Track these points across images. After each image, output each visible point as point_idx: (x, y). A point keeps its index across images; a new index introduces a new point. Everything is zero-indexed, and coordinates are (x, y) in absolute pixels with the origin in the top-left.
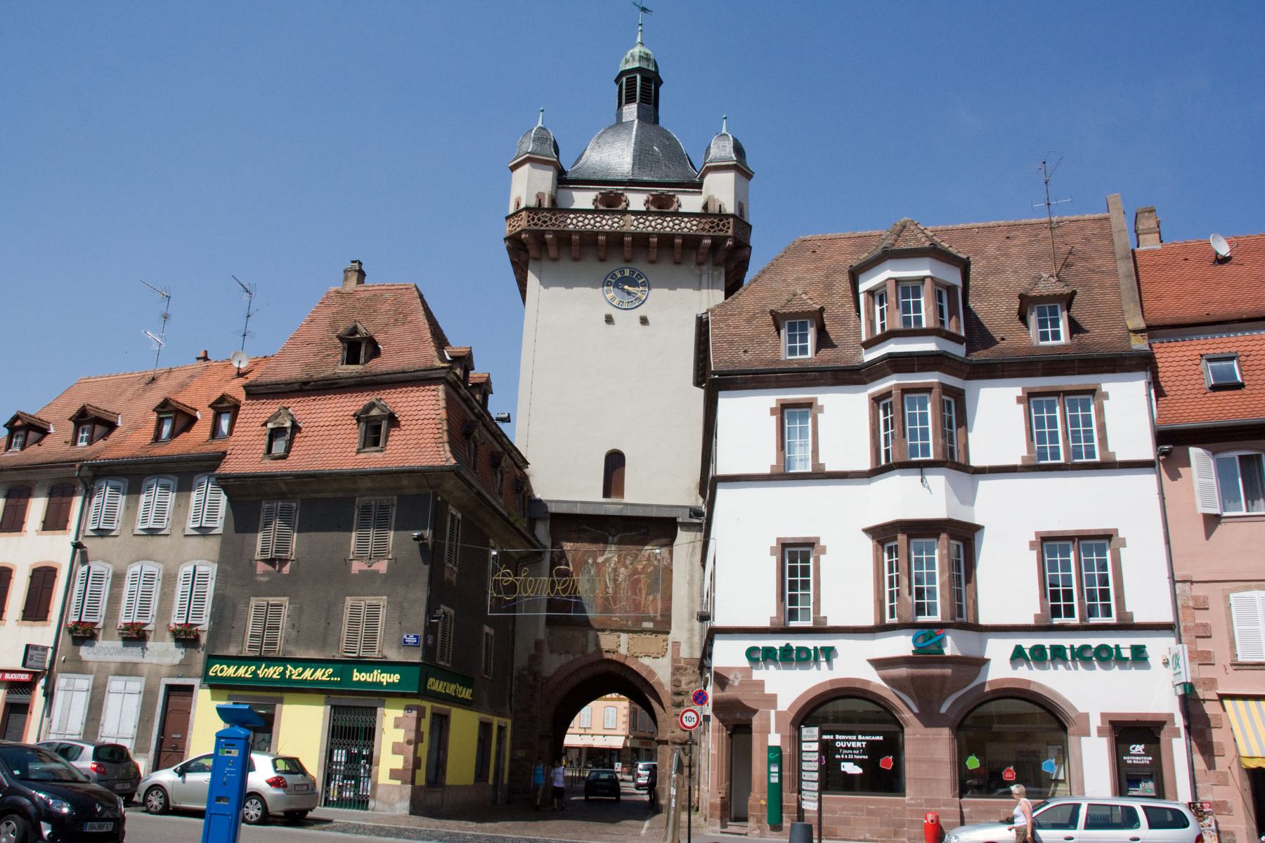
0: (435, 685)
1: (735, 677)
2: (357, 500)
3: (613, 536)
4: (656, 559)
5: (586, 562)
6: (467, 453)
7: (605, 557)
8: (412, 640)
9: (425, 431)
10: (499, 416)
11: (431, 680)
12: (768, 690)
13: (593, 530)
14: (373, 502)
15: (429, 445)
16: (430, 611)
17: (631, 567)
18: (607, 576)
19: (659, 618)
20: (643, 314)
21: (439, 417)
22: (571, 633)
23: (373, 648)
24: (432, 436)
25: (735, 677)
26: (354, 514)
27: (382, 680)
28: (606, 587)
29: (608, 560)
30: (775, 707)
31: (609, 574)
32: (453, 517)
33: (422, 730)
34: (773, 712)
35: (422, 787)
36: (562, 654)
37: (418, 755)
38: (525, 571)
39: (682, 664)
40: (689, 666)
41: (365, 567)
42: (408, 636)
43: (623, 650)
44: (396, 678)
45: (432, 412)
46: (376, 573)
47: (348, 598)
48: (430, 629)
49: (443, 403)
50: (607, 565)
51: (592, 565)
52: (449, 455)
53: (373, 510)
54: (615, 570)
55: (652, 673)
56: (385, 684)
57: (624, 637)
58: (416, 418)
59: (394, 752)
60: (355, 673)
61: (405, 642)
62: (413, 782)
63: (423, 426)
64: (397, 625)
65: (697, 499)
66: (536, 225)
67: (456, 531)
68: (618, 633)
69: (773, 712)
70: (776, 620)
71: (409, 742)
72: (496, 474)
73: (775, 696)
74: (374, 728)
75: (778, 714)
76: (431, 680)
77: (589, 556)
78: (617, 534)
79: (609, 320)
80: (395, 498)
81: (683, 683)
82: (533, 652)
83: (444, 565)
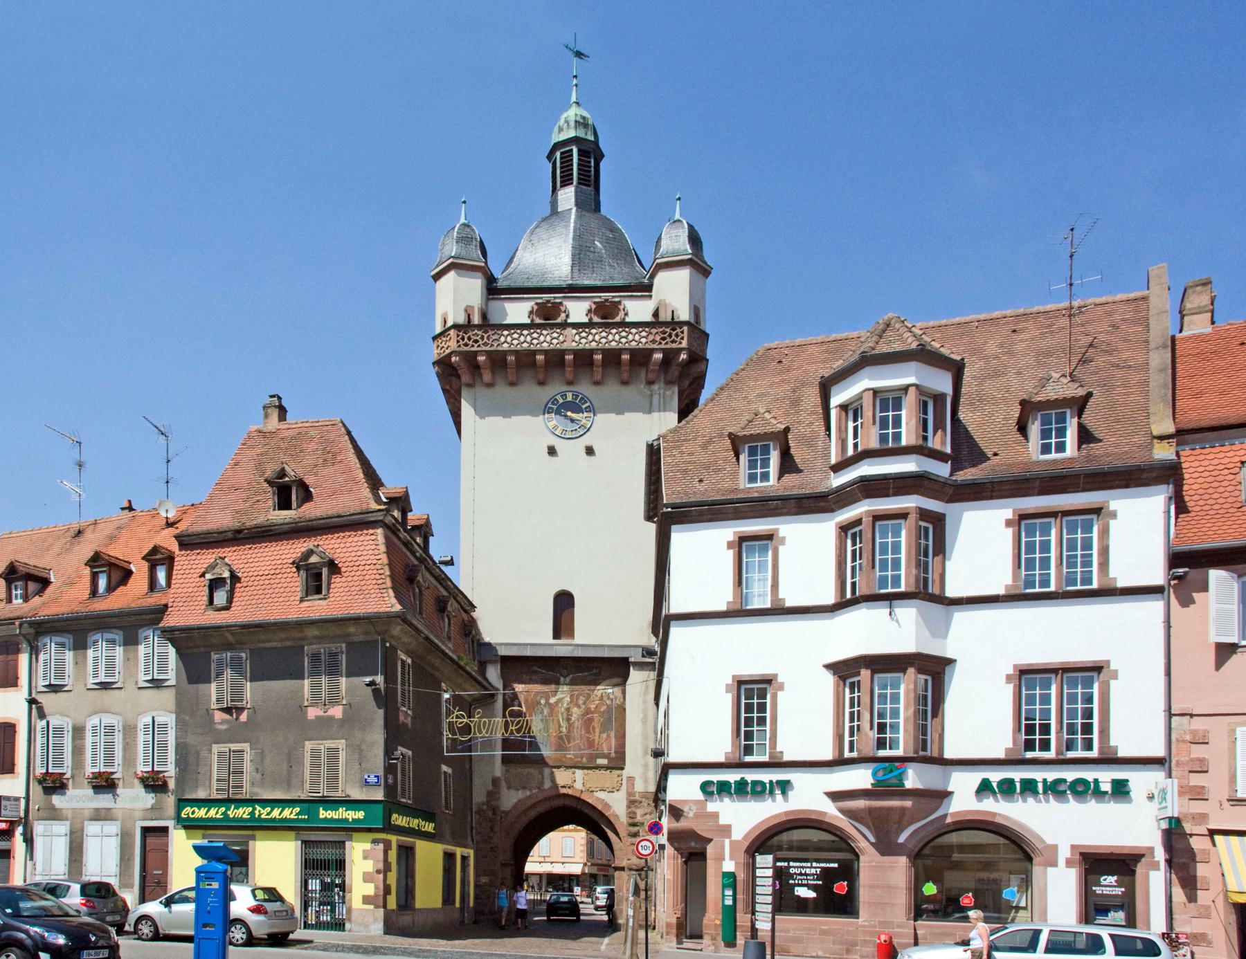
0: (399, 820)
1: (690, 809)
2: (306, 648)
3: (565, 677)
4: (609, 698)
5: (539, 703)
6: (412, 599)
7: (557, 697)
8: (373, 779)
9: (367, 577)
10: (443, 559)
11: (395, 816)
12: (723, 821)
14: (322, 650)
15: (373, 591)
16: (388, 752)
17: (584, 707)
18: (560, 715)
19: (613, 755)
20: (589, 444)
21: (380, 562)
23: (336, 788)
24: (374, 582)
25: (690, 809)
26: (304, 662)
27: (348, 817)
28: (560, 726)
29: (560, 700)
30: (729, 836)
31: (562, 714)
32: (403, 662)
33: (389, 860)
34: (727, 842)
35: (393, 910)
36: (518, 790)
37: (388, 882)
41: (321, 713)
43: (578, 786)
44: (360, 815)
45: (373, 557)
46: (332, 718)
47: (307, 743)
48: (390, 769)
49: (383, 548)
50: (560, 705)
51: (545, 705)
52: (394, 600)
53: (323, 657)
54: (568, 710)
56: (350, 820)
58: (357, 564)
59: (365, 881)
60: (321, 811)
61: (366, 782)
62: (385, 906)
63: (365, 572)
64: (357, 766)
67: (407, 676)
68: (573, 770)
69: (727, 842)
70: (731, 755)
71: (378, 872)
72: (443, 619)
73: (730, 826)
74: (344, 860)
75: (732, 843)
76: (395, 816)
77: (541, 697)
78: (568, 675)
79: (552, 451)
80: (344, 645)
82: (490, 788)
83: (398, 709)
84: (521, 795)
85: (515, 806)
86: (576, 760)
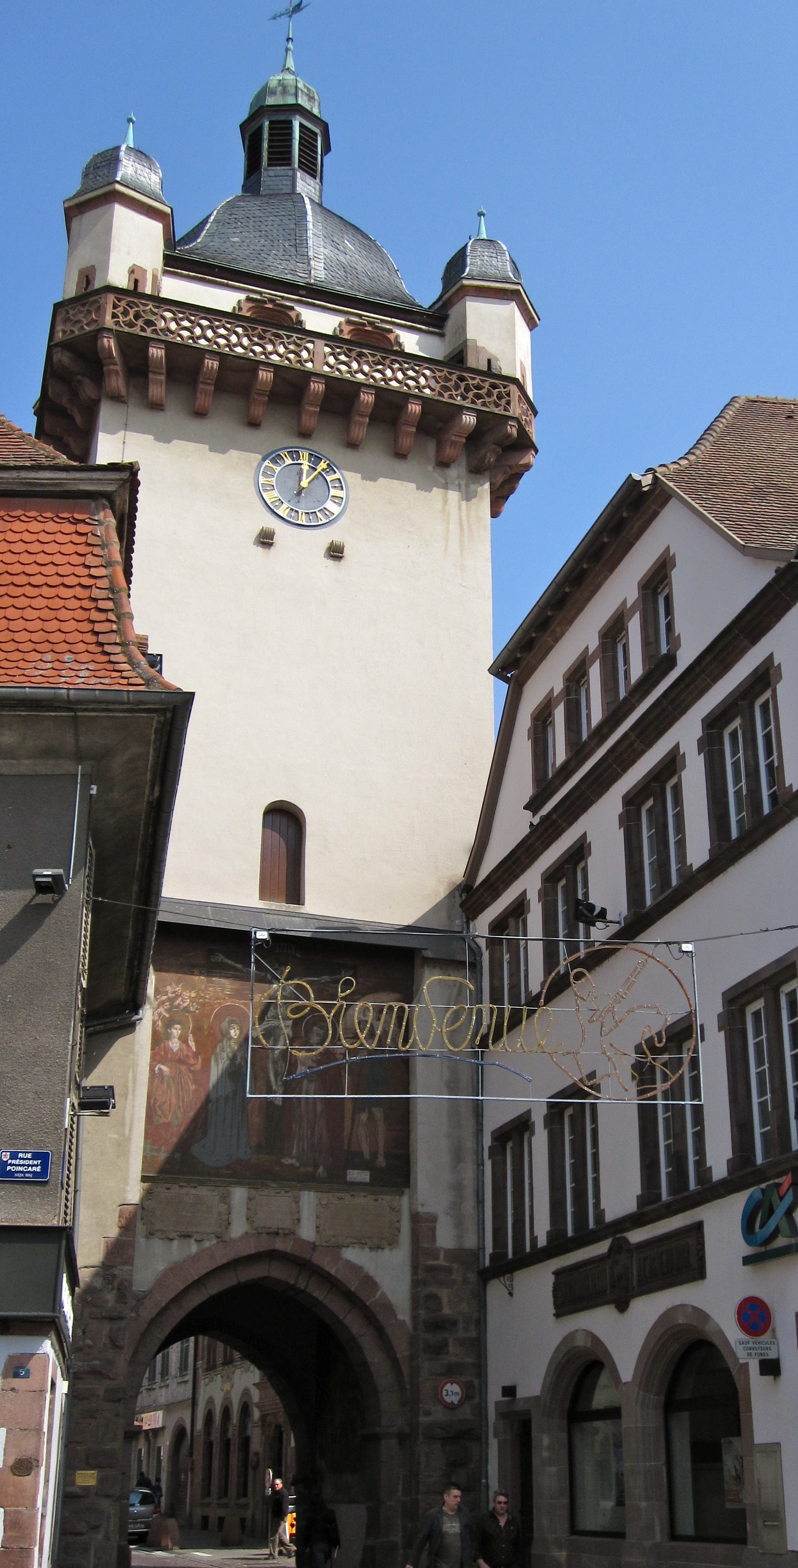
5: (226, 1035)
13: (239, 966)
18: (270, 1066)
19: (381, 1161)
20: (337, 539)
22: (193, 1191)
31: (275, 1062)
36: (172, 1240)
38: (348, 984)
39: (442, 1262)
40: (455, 1266)
42: (14, 1156)
43: (307, 1232)
55: (370, 1282)
57: (308, 1200)
65: (450, 917)
66: (131, 325)
77: (231, 1022)
81: (445, 1300)
84: (177, 1251)
85: (162, 1281)
86: (302, 1169)
